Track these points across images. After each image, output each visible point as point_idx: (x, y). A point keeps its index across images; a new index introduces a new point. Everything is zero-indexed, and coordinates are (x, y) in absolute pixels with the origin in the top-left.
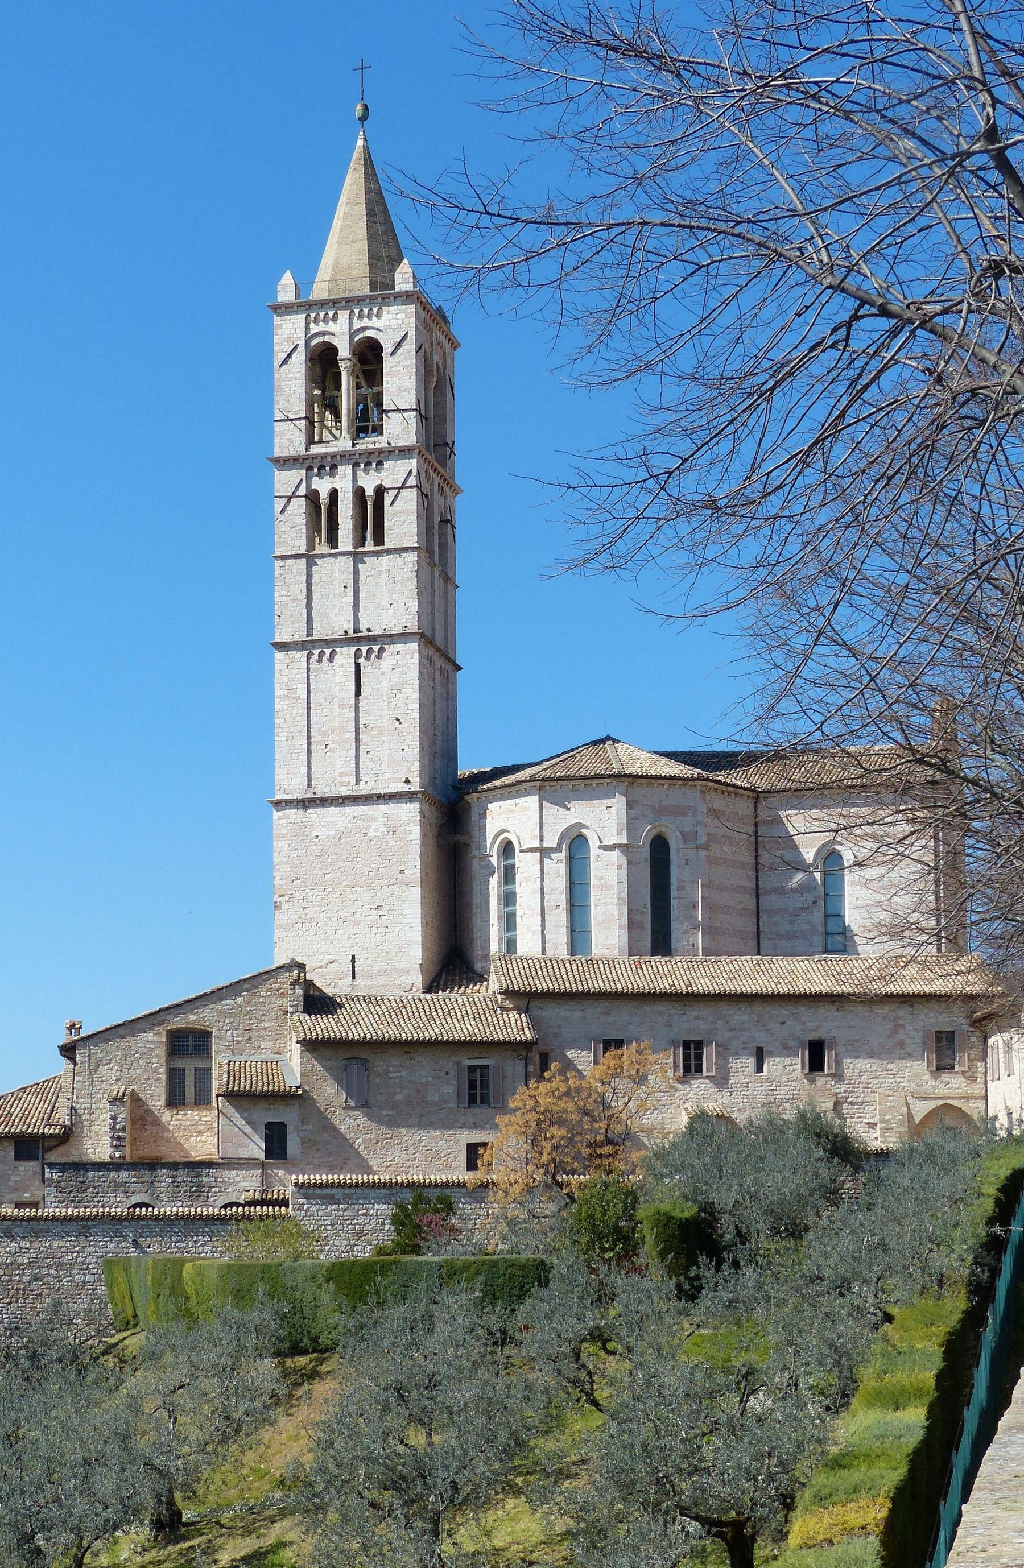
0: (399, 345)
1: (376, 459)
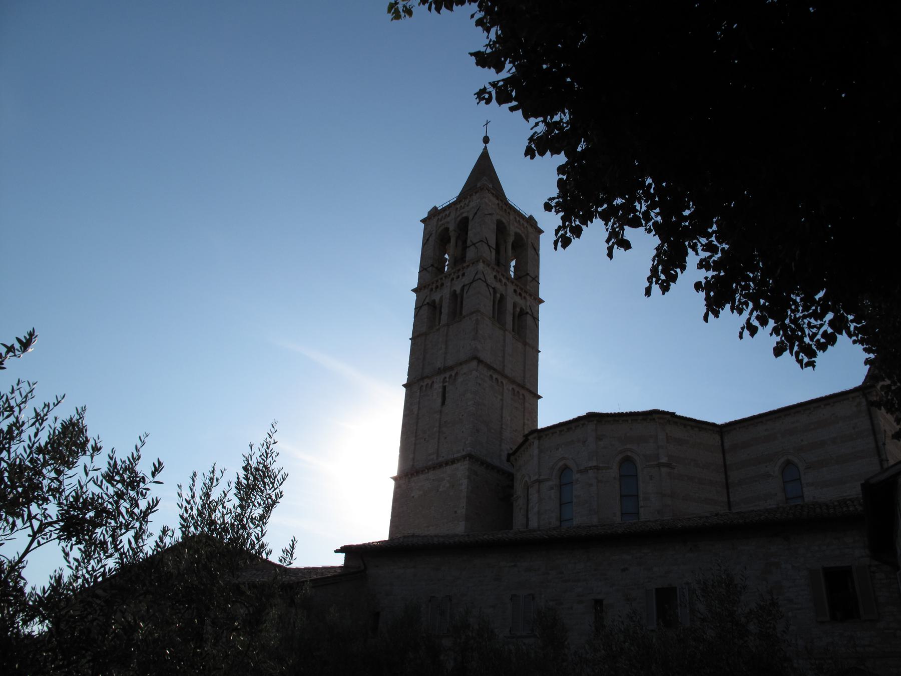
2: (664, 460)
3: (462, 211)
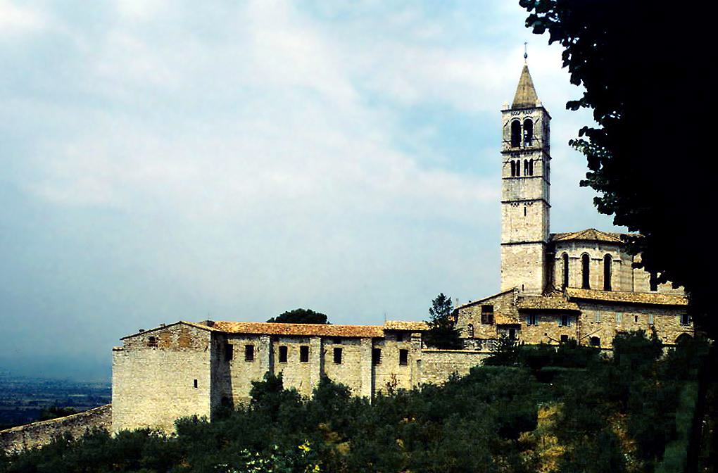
0: (537, 121)
2: (619, 259)
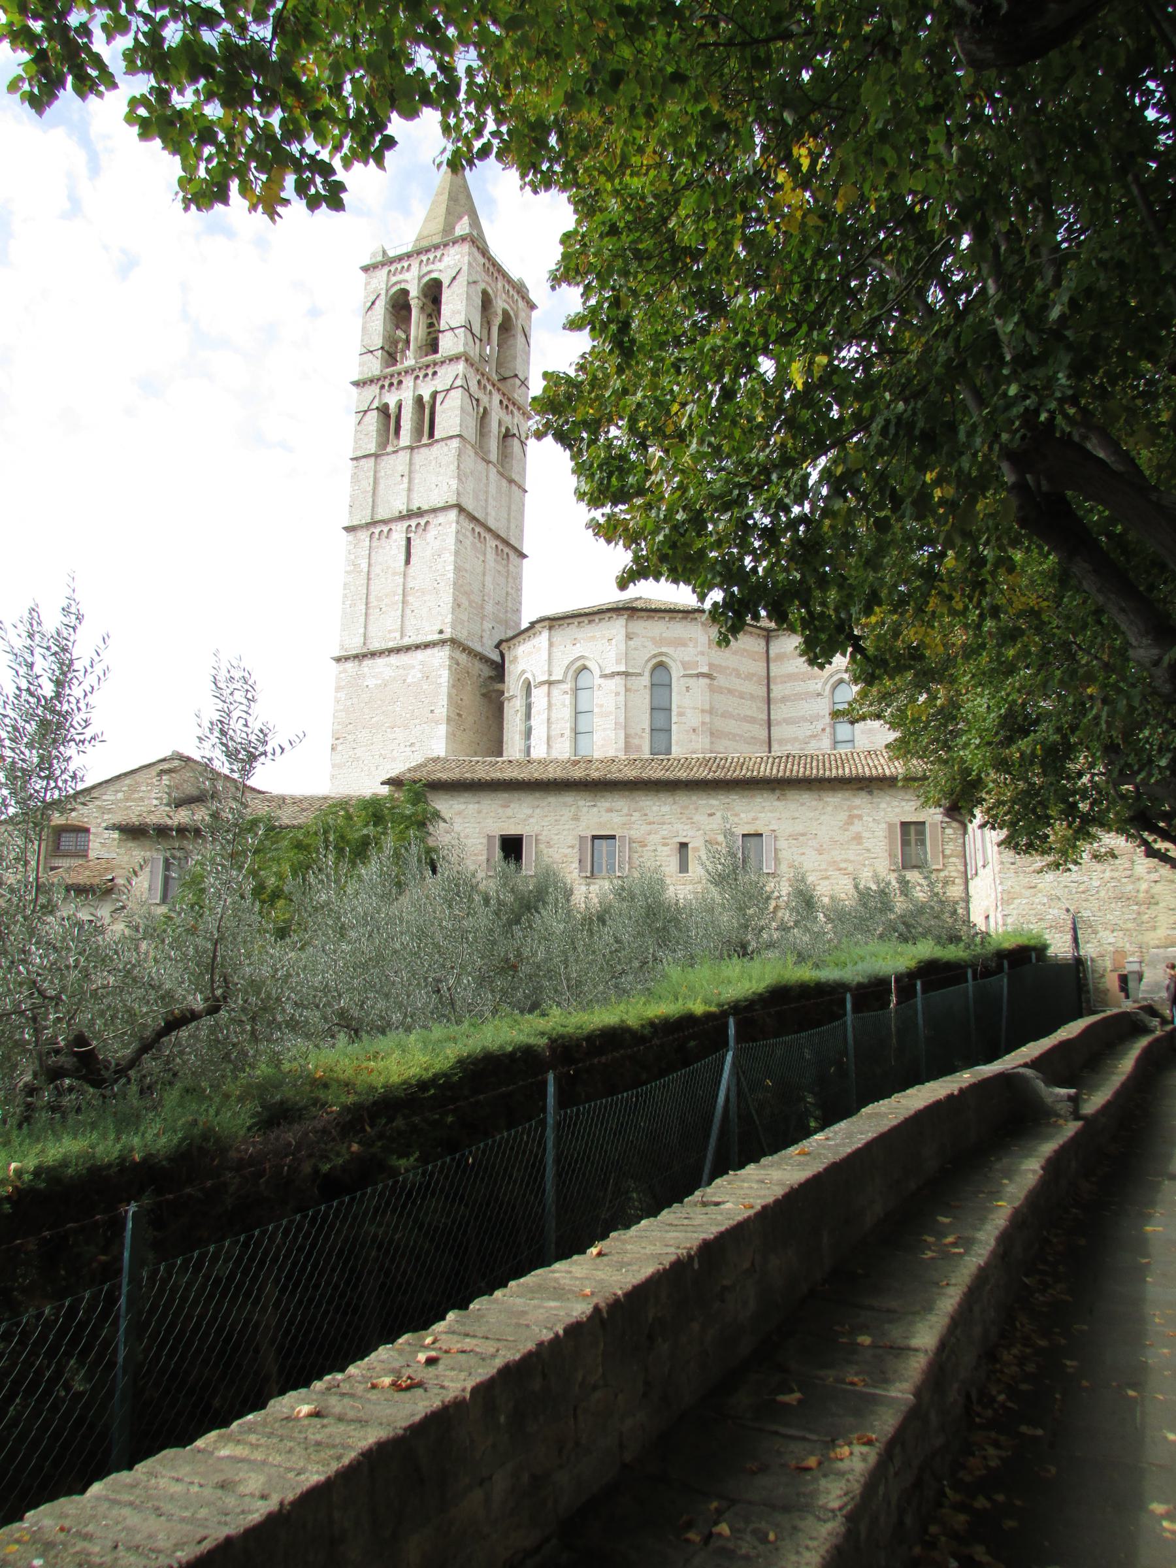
1: (429, 370)
2: (705, 670)
3: (431, 267)
